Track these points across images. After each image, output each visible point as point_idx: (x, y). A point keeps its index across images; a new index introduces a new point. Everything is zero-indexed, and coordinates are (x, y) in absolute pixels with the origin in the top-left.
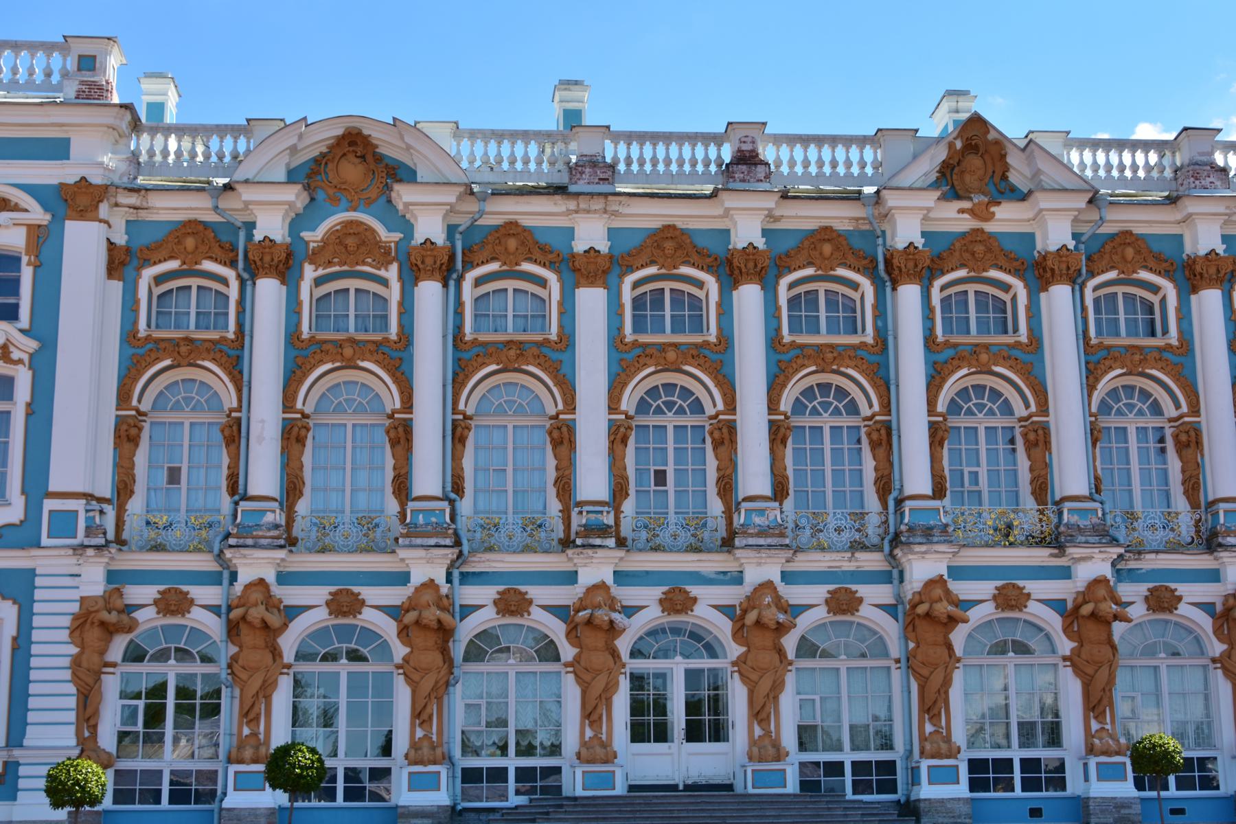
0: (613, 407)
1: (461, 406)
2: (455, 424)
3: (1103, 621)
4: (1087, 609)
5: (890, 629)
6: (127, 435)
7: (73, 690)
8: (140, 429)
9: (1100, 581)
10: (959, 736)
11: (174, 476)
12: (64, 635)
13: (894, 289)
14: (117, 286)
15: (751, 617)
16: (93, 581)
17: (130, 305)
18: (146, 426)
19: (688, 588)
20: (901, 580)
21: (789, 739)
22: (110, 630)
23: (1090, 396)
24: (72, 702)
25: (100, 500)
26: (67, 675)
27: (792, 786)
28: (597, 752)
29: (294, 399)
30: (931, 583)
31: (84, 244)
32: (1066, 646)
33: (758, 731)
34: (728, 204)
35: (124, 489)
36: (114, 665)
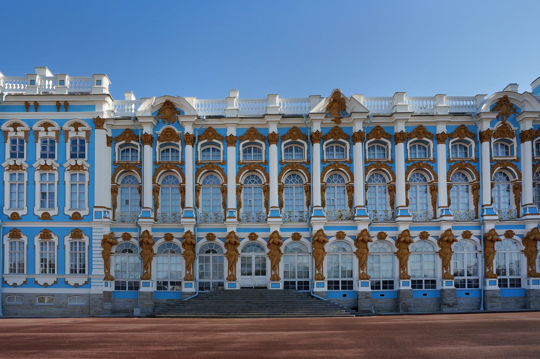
0: (237, 182)
1: (198, 182)
2: (196, 187)
3: (365, 242)
4: (361, 238)
5: (309, 244)
6: (114, 191)
8: (118, 189)
9: (365, 230)
10: (325, 274)
11: (127, 202)
13: (313, 145)
14: (110, 148)
15: (271, 241)
16: (107, 231)
17: (114, 154)
18: (119, 189)
19: (256, 233)
20: (312, 230)
21: (281, 275)
22: (112, 244)
23: (365, 176)
24: (103, 263)
25: (108, 209)
26: (101, 256)
27: (281, 287)
28: (232, 278)
29: (155, 180)
30: (319, 231)
32: (355, 249)
33: (273, 273)
35: (114, 206)
36: (113, 253)
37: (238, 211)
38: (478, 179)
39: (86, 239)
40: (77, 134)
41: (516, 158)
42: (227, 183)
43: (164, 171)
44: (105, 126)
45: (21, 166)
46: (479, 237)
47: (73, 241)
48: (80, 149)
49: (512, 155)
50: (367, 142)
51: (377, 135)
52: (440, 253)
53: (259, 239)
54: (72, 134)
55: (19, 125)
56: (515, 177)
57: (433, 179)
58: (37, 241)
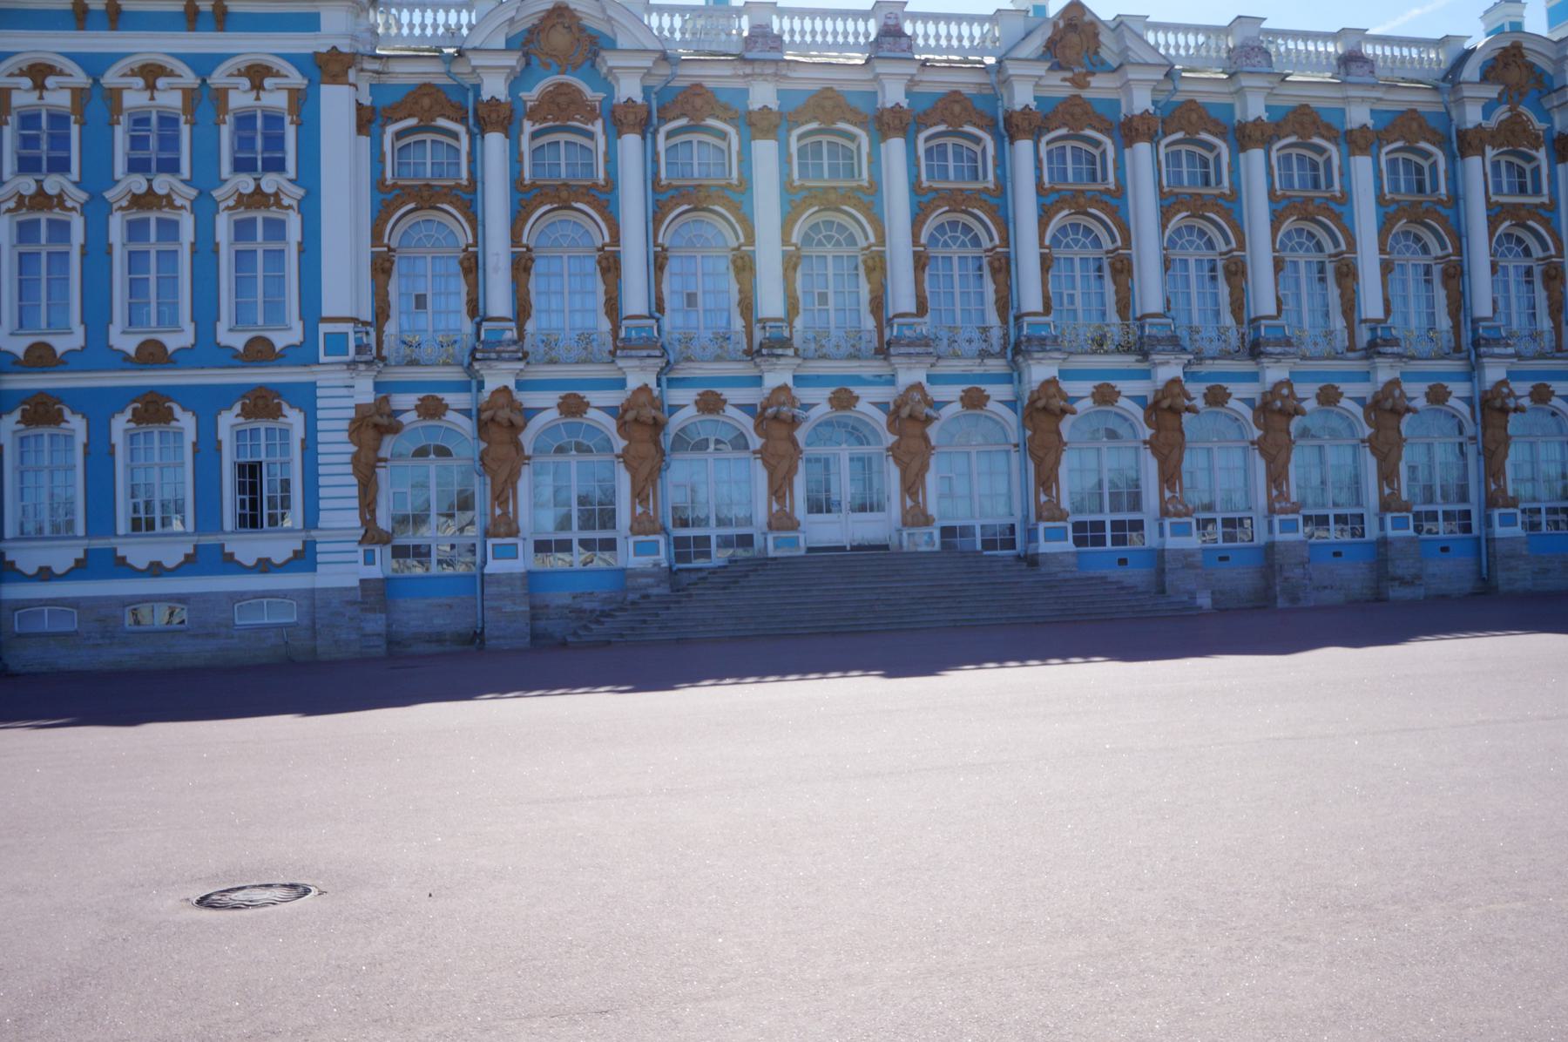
0: (785, 240)
1: (660, 241)
2: (656, 255)
6: (382, 268)
7: (354, 480)
12: (344, 436)
15: (905, 412)
16: (364, 392)
17: (378, 158)
19: (852, 388)
24: (355, 491)
25: (365, 323)
26: (349, 469)
29: (521, 236)
31: (337, 105)
33: (909, 503)
34: (879, 70)
35: (382, 312)
36: (385, 460)
37: (791, 326)
38: (1459, 251)
39: (294, 419)
40: (258, 98)
41: (1545, 200)
42: (752, 243)
43: (548, 207)
44: (352, 75)
45: (60, 197)
46: (1469, 401)
47: (248, 427)
48: (261, 145)
49: (1537, 191)
50: (1164, 142)
51: (1190, 122)
52: (1372, 443)
53: (863, 406)
54: (241, 99)
55: (50, 70)
56: (1545, 247)
57: (1343, 247)
58: (120, 425)
